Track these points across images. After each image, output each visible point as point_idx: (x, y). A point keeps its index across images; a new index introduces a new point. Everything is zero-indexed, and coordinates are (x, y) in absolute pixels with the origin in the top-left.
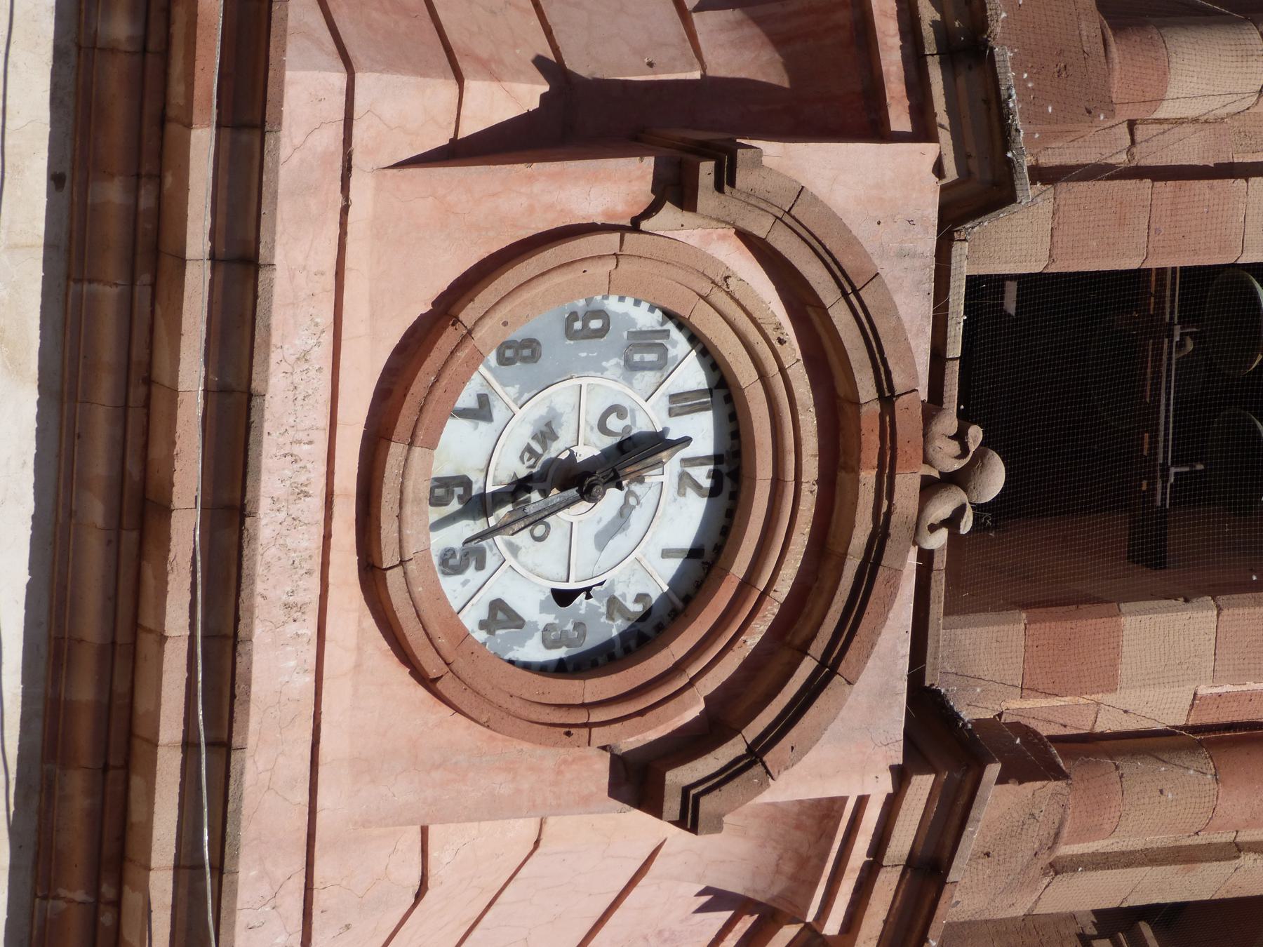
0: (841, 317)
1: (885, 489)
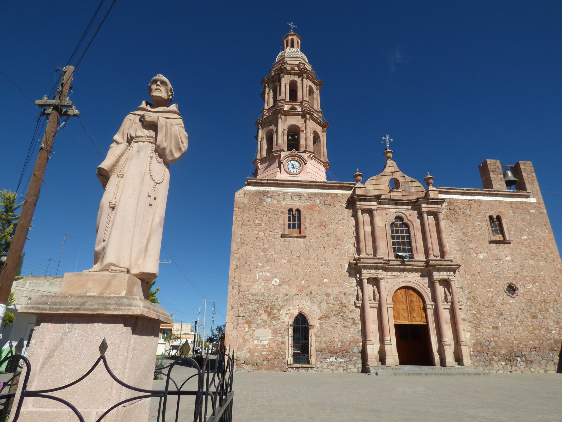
0: (287, 156)
1: (294, 154)
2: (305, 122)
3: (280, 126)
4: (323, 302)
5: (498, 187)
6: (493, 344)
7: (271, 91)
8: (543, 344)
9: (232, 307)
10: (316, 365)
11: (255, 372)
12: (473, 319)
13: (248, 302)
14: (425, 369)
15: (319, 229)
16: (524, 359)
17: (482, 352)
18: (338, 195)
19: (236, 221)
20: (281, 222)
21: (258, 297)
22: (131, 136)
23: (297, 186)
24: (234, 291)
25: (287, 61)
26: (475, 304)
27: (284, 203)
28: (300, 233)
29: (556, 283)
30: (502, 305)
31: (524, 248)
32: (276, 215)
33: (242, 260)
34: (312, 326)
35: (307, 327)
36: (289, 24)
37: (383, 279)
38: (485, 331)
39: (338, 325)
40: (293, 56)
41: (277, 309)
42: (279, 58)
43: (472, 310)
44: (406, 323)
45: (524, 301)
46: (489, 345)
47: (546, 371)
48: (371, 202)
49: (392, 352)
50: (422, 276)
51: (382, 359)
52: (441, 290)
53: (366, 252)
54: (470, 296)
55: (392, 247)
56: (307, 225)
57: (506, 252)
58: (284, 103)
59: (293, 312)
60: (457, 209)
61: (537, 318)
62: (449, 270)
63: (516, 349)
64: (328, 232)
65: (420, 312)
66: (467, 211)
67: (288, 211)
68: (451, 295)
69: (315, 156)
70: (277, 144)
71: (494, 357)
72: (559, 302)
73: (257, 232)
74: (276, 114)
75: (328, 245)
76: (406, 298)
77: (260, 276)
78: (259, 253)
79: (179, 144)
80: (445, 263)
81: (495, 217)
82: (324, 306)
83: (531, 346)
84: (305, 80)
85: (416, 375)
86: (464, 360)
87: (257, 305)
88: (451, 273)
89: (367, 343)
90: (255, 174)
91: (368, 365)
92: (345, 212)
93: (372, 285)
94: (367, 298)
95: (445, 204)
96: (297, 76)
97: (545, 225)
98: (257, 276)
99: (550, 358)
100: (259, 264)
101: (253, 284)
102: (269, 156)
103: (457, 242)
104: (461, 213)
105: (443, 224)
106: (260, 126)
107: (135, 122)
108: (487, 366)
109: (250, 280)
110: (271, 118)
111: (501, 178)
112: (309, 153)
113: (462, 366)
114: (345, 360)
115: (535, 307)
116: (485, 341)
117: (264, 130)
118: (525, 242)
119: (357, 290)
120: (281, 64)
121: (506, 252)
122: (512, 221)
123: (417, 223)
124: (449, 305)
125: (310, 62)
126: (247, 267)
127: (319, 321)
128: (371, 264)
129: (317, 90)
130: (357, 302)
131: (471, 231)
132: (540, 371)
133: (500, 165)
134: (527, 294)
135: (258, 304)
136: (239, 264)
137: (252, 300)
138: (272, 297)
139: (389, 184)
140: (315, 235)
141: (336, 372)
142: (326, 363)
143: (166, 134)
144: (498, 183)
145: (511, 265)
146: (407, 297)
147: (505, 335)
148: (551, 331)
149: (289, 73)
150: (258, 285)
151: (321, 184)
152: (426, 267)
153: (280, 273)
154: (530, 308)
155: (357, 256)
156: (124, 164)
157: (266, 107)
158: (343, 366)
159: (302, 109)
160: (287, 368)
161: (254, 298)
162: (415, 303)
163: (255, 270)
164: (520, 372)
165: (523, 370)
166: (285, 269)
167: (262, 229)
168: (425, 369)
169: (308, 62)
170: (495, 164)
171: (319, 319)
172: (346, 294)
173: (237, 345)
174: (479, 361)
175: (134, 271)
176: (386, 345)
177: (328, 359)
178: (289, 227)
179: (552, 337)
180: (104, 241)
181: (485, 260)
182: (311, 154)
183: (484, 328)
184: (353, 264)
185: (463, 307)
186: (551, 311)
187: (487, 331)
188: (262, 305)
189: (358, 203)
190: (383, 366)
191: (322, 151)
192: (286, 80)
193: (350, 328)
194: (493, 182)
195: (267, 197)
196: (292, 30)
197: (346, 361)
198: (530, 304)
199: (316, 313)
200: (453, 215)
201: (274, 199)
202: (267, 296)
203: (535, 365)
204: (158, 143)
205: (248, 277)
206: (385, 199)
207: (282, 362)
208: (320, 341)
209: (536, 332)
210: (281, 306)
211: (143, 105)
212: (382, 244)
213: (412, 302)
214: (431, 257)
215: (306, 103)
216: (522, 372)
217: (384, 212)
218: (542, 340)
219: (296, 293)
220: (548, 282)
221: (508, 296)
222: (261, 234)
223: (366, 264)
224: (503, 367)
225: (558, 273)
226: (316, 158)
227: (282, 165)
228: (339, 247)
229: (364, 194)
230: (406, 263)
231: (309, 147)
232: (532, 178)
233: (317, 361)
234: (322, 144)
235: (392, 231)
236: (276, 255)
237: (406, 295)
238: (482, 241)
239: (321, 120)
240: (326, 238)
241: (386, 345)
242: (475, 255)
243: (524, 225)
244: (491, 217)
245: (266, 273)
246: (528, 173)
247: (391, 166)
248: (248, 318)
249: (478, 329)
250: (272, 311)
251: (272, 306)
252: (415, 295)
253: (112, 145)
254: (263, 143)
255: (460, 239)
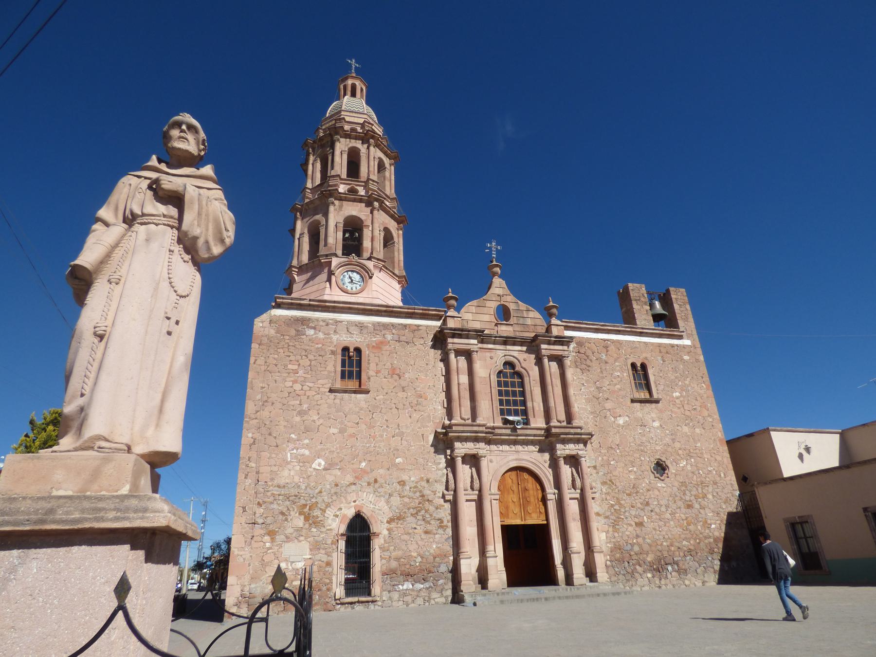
1: (353, 262)
2: (372, 212)
3: (331, 216)
4: (394, 495)
5: (643, 322)
6: (636, 548)
7: (319, 161)
8: (701, 544)
9: (244, 508)
10: (381, 596)
11: (281, 615)
12: (610, 513)
13: (272, 499)
14: (545, 591)
15: (390, 380)
16: (676, 567)
17: (621, 561)
18: (420, 328)
19: (255, 365)
20: (330, 368)
21: (289, 491)
22: (132, 213)
23: (357, 311)
24: (249, 481)
25: (345, 117)
26: (612, 490)
27: (335, 337)
28: (360, 386)
29: (717, 458)
30: (649, 490)
31: (676, 410)
32: (322, 356)
33: (264, 430)
34: (376, 534)
35: (369, 535)
36: (349, 61)
37: (485, 457)
38: (625, 530)
39: (417, 530)
40: (354, 109)
41: (321, 509)
42: (333, 112)
43: (609, 500)
44: (518, 522)
45: (676, 484)
46: (632, 550)
47: (704, 583)
48: (469, 340)
49: (497, 567)
50: (541, 451)
51: (483, 580)
52: (566, 471)
53: (460, 415)
54: (607, 479)
55: (499, 407)
56: (371, 373)
57: (653, 415)
58: (339, 180)
59: (346, 513)
60: (589, 353)
61: (692, 508)
62: (578, 441)
63: (665, 554)
64: (404, 383)
65: (538, 506)
66: (602, 356)
67: (342, 350)
68: (580, 478)
69: (386, 266)
70: (326, 244)
71: (638, 567)
72: (720, 485)
73: (290, 384)
74: (326, 197)
75: (404, 405)
76: (518, 484)
77: (293, 456)
78: (293, 417)
79: (220, 233)
80: (572, 431)
81: (639, 365)
82: (396, 501)
83: (685, 549)
84: (372, 148)
85: (532, 600)
86: (598, 575)
87: (288, 503)
88: (581, 446)
89: (461, 557)
90: (289, 290)
91: (462, 591)
92: (430, 354)
93: (469, 466)
94: (461, 486)
95: (573, 345)
96: (361, 142)
97: (702, 377)
98: (287, 456)
99: (709, 564)
100: (291, 435)
101: (281, 469)
102: (313, 262)
103: (588, 401)
104: (595, 358)
105: (570, 374)
106: (298, 214)
107: (140, 191)
108: (628, 580)
109: (276, 462)
110: (317, 202)
111: (647, 311)
112: (376, 261)
113: (595, 584)
114: (427, 585)
115: (690, 492)
116: (625, 545)
117: (305, 220)
118: (678, 401)
119: (447, 474)
120: (335, 120)
121: (653, 415)
122: (661, 371)
123: (535, 371)
124: (577, 493)
125: (381, 122)
126: (271, 441)
127: (388, 525)
128: (469, 434)
129: (390, 165)
130: (446, 492)
131: (608, 385)
132: (696, 582)
133: (645, 292)
134: (680, 475)
135: (289, 501)
136: (257, 435)
137: (279, 495)
138: (312, 489)
139: (495, 313)
140: (383, 389)
141: (413, 605)
142: (397, 592)
143: (199, 214)
144: (643, 317)
145: (659, 433)
146: (520, 483)
147: (653, 534)
148: (709, 526)
149: (347, 136)
150: (289, 470)
151: (394, 309)
152: (547, 437)
153: (327, 450)
154: (683, 495)
155: (447, 422)
156: (121, 260)
157: (309, 185)
158: (423, 595)
159: (367, 192)
160: (334, 606)
161: (283, 492)
162: (531, 492)
163: (285, 445)
164: (672, 586)
165: (675, 583)
166: (335, 443)
167: (299, 378)
168: (545, 591)
169: (377, 122)
170: (640, 291)
171: (388, 522)
172: (430, 481)
173: (251, 572)
174: (618, 575)
175: (140, 449)
176: (489, 557)
177: (400, 586)
178: (343, 377)
179: (711, 534)
180: (82, 395)
181: (626, 425)
182: (379, 262)
183: (625, 526)
184: (442, 434)
185: (597, 495)
186: (710, 497)
187: (629, 530)
188: (296, 503)
189: (450, 340)
190: (484, 591)
191: (396, 260)
192: (342, 146)
193: (435, 534)
194: (636, 315)
195: (308, 327)
196: (353, 71)
197: (428, 586)
198: (683, 488)
199: (383, 513)
200: (583, 363)
201: (320, 331)
202: (303, 487)
203: (689, 575)
204: (184, 227)
205: (272, 458)
206: (490, 336)
207: (327, 596)
208: (388, 557)
209: (692, 527)
210: (327, 504)
211: (154, 161)
212: (485, 404)
213: (526, 490)
214: (554, 423)
215: (373, 184)
216: (674, 587)
217: (488, 355)
218: (698, 539)
219: (352, 482)
220: (705, 457)
221: (655, 477)
222: (298, 387)
223: (460, 434)
224: (649, 581)
225: (718, 444)
226: (386, 268)
227: (333, 278)
228: (420, 407)
229: (459, 327)
230: (519, 432)
231: (377, 251)
232: (686, 312)
233: (382, 590)
234: (396, 248)
235: (499, 384)
236: (320, 420)
237: (518, 480)
238: (622, 398)
239: (396, 212)
240: (401, 395)
241: (489, 557)
242: (613, 419)
243: (676, 377)
244: (634, 365)
245: (304, 450)
246: (681, 305)
247: (499, 286)
248: (271, 526)
249: (617, 527)
250: (311, 512)
251: (312, 505)
252: (531, 480)
253: (95, 227)
254: (303, 241)
255: (593, 396)
